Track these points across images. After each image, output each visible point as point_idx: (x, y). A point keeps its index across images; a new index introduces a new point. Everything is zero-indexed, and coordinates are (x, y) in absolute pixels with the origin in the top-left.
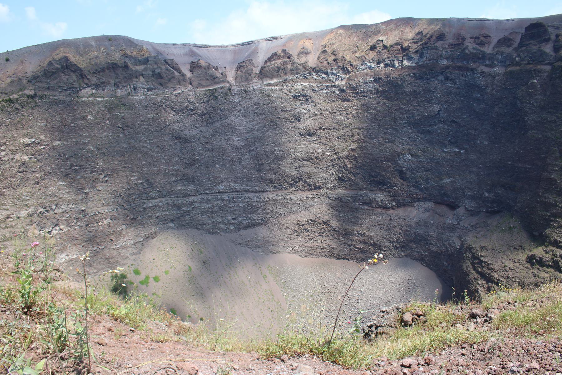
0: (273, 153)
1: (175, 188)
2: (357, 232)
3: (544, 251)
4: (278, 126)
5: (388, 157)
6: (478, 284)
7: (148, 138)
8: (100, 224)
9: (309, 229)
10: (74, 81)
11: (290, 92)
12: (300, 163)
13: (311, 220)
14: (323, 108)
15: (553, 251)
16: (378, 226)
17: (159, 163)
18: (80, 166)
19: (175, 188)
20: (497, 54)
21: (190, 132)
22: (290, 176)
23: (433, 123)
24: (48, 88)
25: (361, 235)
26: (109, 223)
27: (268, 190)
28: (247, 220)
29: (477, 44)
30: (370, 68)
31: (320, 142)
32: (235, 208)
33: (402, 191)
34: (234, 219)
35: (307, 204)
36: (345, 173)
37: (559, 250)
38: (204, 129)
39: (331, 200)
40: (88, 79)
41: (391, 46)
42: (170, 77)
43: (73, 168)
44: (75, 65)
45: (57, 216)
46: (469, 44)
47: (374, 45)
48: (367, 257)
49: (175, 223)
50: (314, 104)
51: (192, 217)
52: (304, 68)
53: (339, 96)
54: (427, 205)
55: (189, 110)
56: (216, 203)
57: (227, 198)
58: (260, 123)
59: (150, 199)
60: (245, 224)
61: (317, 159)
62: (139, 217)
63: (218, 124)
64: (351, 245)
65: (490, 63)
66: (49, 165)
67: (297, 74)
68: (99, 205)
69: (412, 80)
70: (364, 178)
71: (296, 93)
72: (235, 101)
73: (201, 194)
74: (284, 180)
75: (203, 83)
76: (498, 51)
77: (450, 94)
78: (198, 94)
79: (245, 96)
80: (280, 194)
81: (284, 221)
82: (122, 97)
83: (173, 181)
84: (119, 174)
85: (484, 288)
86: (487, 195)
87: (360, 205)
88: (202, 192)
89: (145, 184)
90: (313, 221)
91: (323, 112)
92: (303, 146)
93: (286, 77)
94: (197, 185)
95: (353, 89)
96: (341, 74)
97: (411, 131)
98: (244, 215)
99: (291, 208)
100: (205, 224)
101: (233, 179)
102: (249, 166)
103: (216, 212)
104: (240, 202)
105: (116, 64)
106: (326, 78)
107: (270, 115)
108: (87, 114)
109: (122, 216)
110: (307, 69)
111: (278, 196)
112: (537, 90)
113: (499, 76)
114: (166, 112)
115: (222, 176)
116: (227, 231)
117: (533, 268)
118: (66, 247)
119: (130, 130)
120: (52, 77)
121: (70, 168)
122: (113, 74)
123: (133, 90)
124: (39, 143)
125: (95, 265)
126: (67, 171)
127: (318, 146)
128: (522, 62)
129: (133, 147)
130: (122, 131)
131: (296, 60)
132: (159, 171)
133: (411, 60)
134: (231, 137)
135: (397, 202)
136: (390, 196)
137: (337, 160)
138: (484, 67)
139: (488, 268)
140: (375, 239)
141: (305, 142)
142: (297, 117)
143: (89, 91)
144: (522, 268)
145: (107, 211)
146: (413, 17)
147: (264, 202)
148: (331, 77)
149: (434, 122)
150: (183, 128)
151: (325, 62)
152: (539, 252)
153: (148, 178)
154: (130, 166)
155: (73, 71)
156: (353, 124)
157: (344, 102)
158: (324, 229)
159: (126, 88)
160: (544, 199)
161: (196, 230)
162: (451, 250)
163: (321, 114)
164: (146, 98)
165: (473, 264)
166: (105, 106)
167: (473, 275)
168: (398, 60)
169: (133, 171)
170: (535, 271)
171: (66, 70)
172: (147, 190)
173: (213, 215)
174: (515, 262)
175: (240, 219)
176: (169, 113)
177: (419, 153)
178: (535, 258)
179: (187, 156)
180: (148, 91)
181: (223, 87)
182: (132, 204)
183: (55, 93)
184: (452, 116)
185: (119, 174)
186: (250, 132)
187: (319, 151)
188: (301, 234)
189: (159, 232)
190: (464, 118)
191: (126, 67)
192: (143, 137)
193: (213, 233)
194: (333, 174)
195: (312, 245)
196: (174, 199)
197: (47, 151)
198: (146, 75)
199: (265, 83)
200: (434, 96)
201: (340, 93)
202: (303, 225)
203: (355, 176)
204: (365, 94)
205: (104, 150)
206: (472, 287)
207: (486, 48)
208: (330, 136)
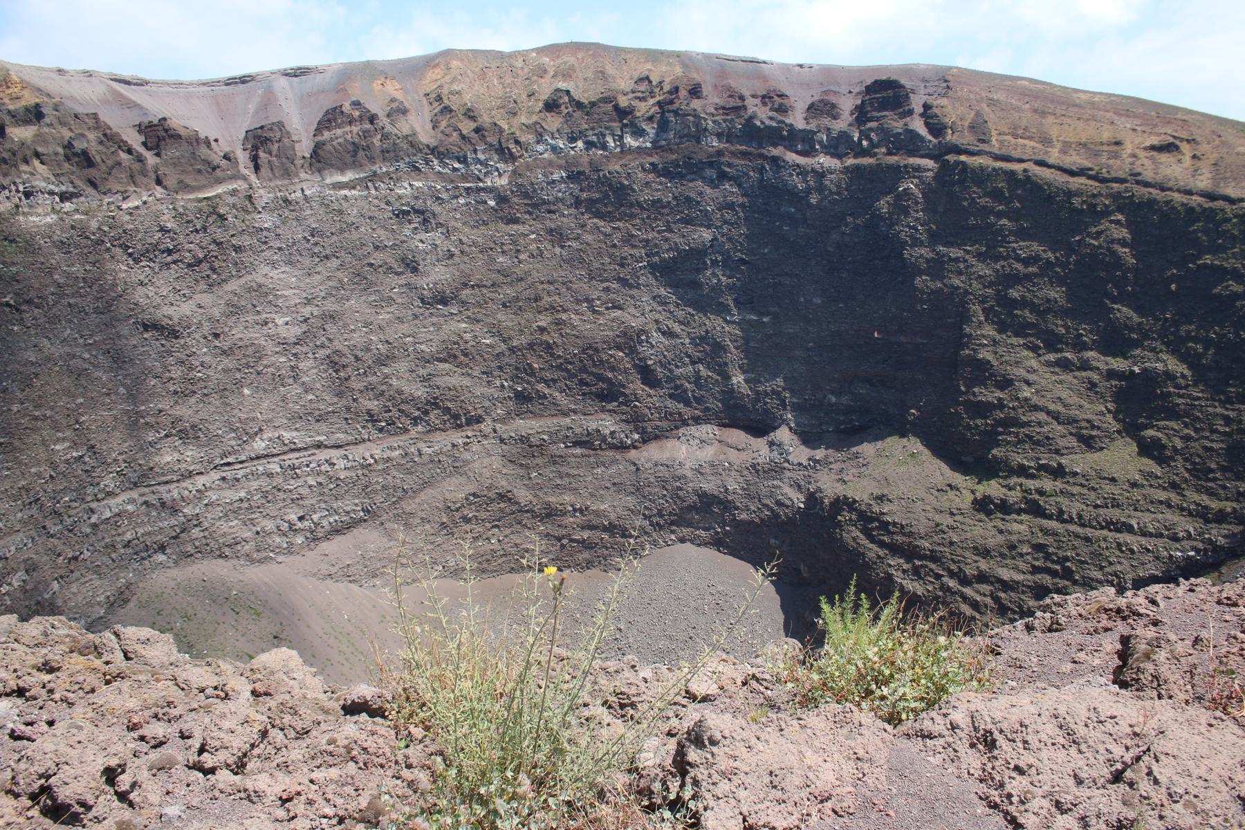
0: (368, 350)
1: (157, 459)
2: (572, 506)
3: (1003, 486)
4: (371, 284)
5: (618, 339)
6: (890, 566)
7: (79, 332)
9: (470, 515)
11: (388, 203)
12: (430, 369)
13: (474, 495)
14: (465, 239)
15: (1021, 485)
16: (615, 489)
17: (113, 397)
20: (818, 132)
22: (413, 400)
23: (701, 266)
25: (581, 511)
26: (24, 581)
27: (366, 437)
28: (330, 515)
29: (771, 109)
30: (554, 149)
31: (469, 317)
32: (301, 491)
33: (650, 408)
34: (301, 518)
35: (456, 459)
36: (529, 382)
37: (1032, 482)
38: (206, 299)
39: (506, 444)
41: (593, 104)
46: (755, 109)
47: (554, 100)
48: (599, 557)
49: (168, 551)
50: (445, 231)
52: (412, 146)
53: (496, 211)
54: (704, 431)
56: (255, 485)
57: (279, 470)
58: (329, 278)
59: (103, 499)
60: (328, 528)
61: (466, 355)
62: (85, 552)
63: (233, 285)
64: (563, 537)
65: (807, 147)
67: (398, 161)
69: (651, 176)
70: (569, 389)
71: (403, 205)
72: (266, 225)
73: (215, 468)
74: (399, 410)
75: (189, 180)
76: (818, 126)
77: (731, 206)
78: (181, 210)
79: (287, 213)
80: (396, 445)
81: (414, 506)
84: (26, 441)
85: (904, 571)
86: (834, 399)
87: (567, 447)
88: (218, 461)
89: (87, 459)
90: (478, 497)
91: (467, 249)
92: (431, 329)
93: (374, 168)
94: (206, 446)
95: (526, 195)
96: (496, 163)
97: (654, 282)
98: (323, 505)
99: (422, 473)
101: (285, 421)
102: (318, 385)
103: (258, 507)
104: (309, 475)
106: (463, 171)
107: (349, 258)
109: (46, 558)
110: (420, 150)
111: (391, 448)
112: (917, 203)
113: (831, 173)
116: (290, 550)
117: (991, 520)
127: (464, 325)
128: (876, 150)
129: (48, 359)
130: (17, 316)
131: (389, 128)
133: (641, 136)
134: (268, 316)
135: (643, 432)
136: (627, 422)
137: (507, 353)
138: (794, 155)
139: (904, 534)
140: (613, 516)
141: (434, 319)
142: (408, 261)
144: (971, 521)
146: (601, 42)
147: (363, 467)
148: (476, 169)
149: (705, 263)
151: (455, 134)
152: (993, 489)
154: (49, 413)
156: (535, 273)
157: (507, 224)
158: (501, 510)
160: (972, 398)
161: (221, 561)
162: (785, 513)
163: (462, 252)
167: (873, 551)
168: (613, 135)
169: (56, 427)
170: (999, 524)
172: (94, 474)
173: (253, 516)
174: (952, 514)
175: (315, 517)
177: (677, 328)
178: (992, 502)
179: (176, 373)
180: (62, 201)
181: (234, 193)
182: (66, 517)
184: (740, 251)
186: (308, 302)
187: (468, 336)
188: (455, 530)
189: (136, 583)
190: (765, 254)
192: (68, 331)
194: (503, 386)
195: (481, 550)
196: (162, 488)
199: (328, 181)
200: (700, 211)
201: (497, 204)
202: (457, 510)
203: (549, 387)
204: (553, 208)
206: (877, 574)
207: (791, 117)
208: (486, 303)
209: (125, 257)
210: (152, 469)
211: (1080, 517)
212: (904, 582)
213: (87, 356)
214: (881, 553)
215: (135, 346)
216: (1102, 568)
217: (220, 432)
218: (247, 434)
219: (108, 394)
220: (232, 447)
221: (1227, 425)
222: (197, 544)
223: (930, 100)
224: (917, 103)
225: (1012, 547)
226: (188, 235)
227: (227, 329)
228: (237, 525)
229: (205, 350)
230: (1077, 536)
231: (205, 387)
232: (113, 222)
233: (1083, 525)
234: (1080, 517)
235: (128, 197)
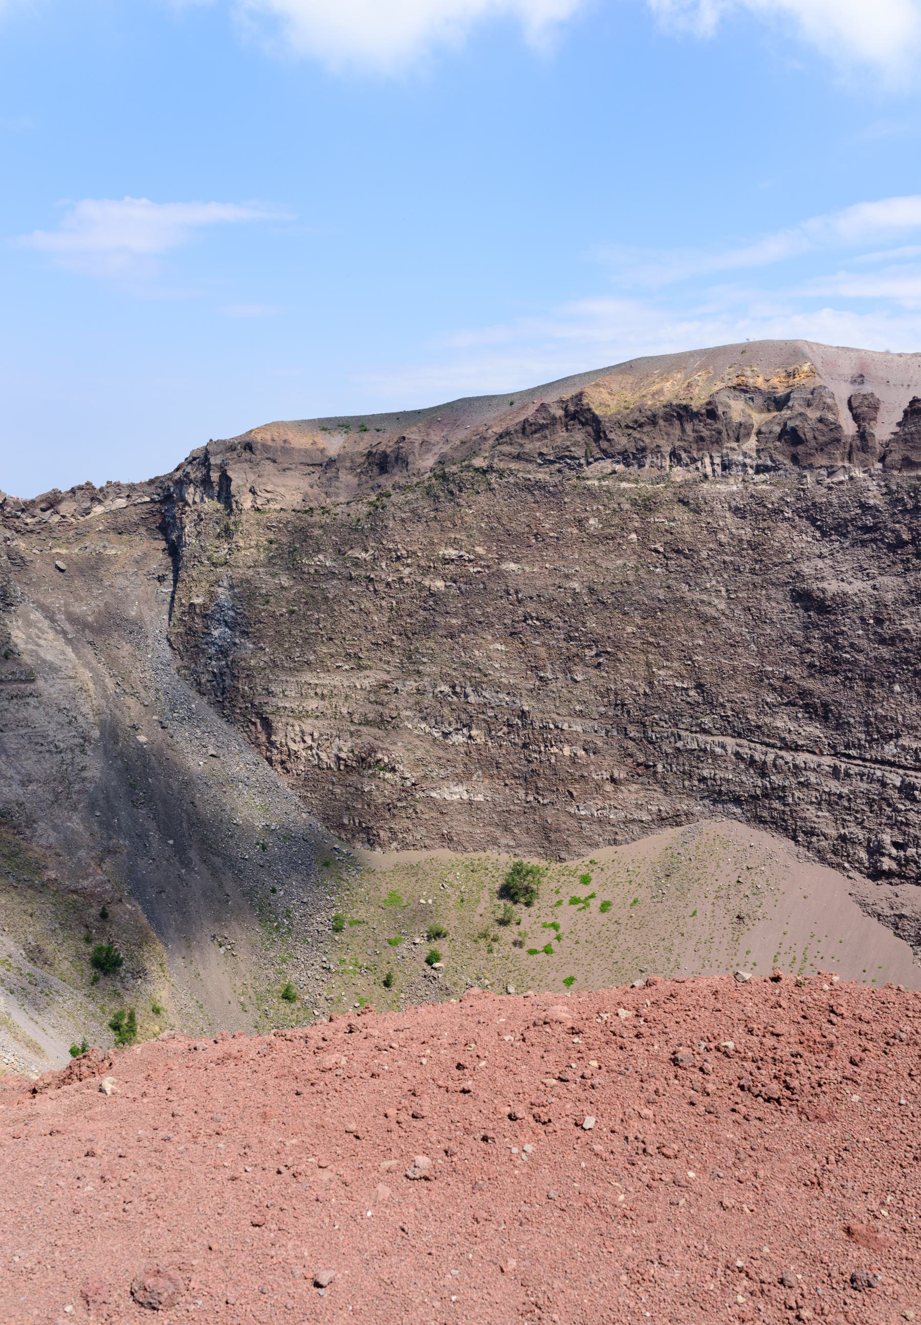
1: (768, 720)
8: (554, 750)
10: (574, 445)
17: (740, 650)
18: (543, 620)
19: (768, 720)
21: (844, 584)
24: (518, 457)
40: (609, 440)
42: (822, 439)
43: (530, 622)
44: (589, 410)
45: (470, 708)
49: (745, 807)
51: (788, 805)
55: (860, 528)
56: (864, 786)
57: (898, 784)
59: (696, 732)
66: (480, 606)
68: (563, 711)
82: (686, 484)
83: (767, 703)
88: (841, 749)
94: (834, 730)
100: (818, 835)
103: (857, 812)
105: (686, 408)
108: (587, 514)
109: (616, 751)
114: (794, 527)
115: (900, 718)
118: (472, 774)
119: (684, 560)
120: (537, 435)
121: (525, 621)
122: (678, 432)
123: (719, 469)
124: (470, 561)
125: (516, 831)
126: (516, 625)
132: (734, 669)
143: (607, 465)
145: (579, 729)
150: (828, 572)
153: (702, 681)
154: (662, 643)
155: (583, 424)
159: (699, 464)
161: (793, 843)
164: (746, 488)
166: (634, 503)
171: (572, 422)
172: (696, 709)
173: (847, 818)
176: (801, 532)
183: (530, 467)
185: (632, 657)
191: (712, 414)
192: (714, 582)
193: (831, 865)
197: (484, 579)
198: (765, 433)
205: (605, 596)
209: (813, 529)
210: (759, 727)
213: (722, 606)
215: (783, 611)
217: (852, 720)
218: (879, 732)
219: (731, 645)
220: (859, 740)
222: (775, 814)
226: (894, 513)
227: (896, 617)
228: (825, 817)
229: (861, 632)
231: (850, 671)
232: (801, 493)
235: (834, 472)
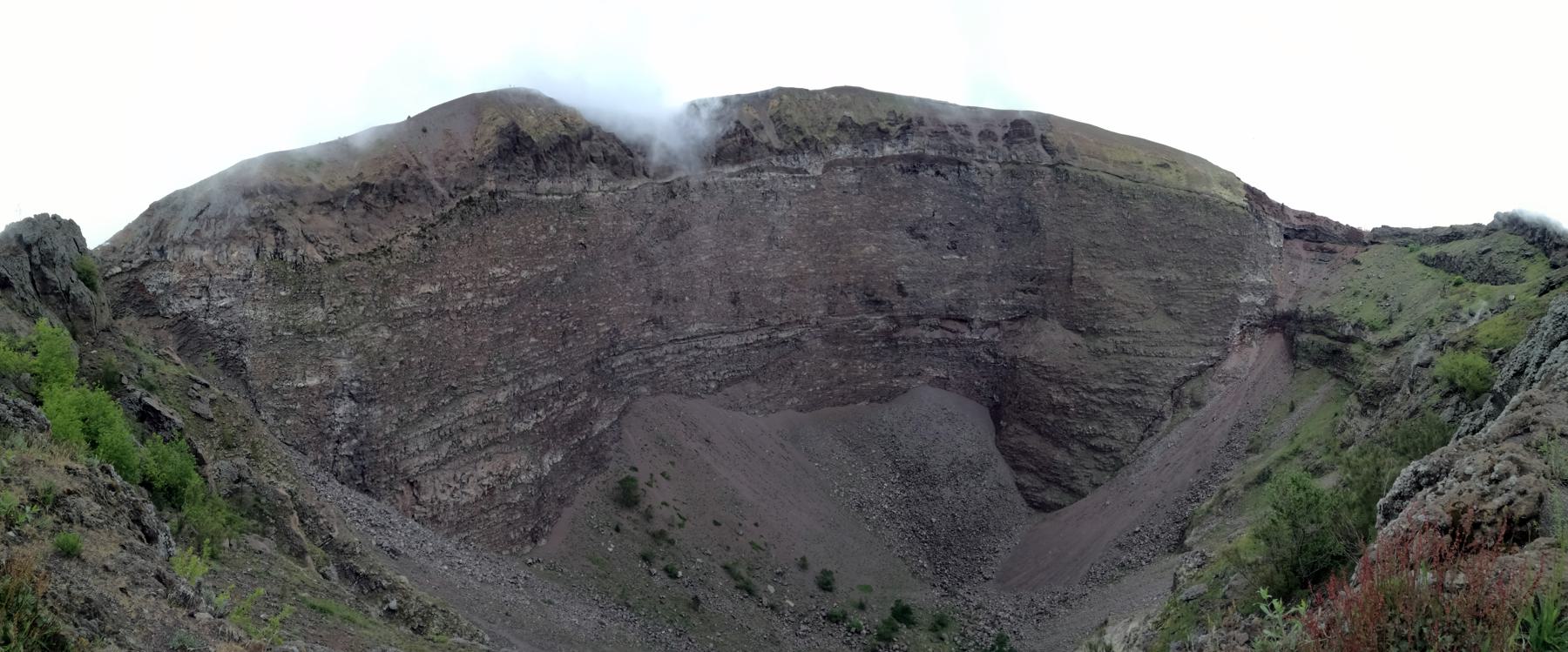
86: (1004, 302)
88: (672, 338)
139: (1055, 372)
161: (673, 395)
165: (1035, 373)
175: (722, 373)
211: (1145, 352)
212: (1059, 398)
214: (1043, 384)
216: (1159, 376)
221: (1208, 300)
223: (1044, 133)
224: (1038, 133)
225: (1113, 372)
230: (1145, 362)
233: (1148, 356)
234: (1145, 352)
